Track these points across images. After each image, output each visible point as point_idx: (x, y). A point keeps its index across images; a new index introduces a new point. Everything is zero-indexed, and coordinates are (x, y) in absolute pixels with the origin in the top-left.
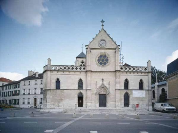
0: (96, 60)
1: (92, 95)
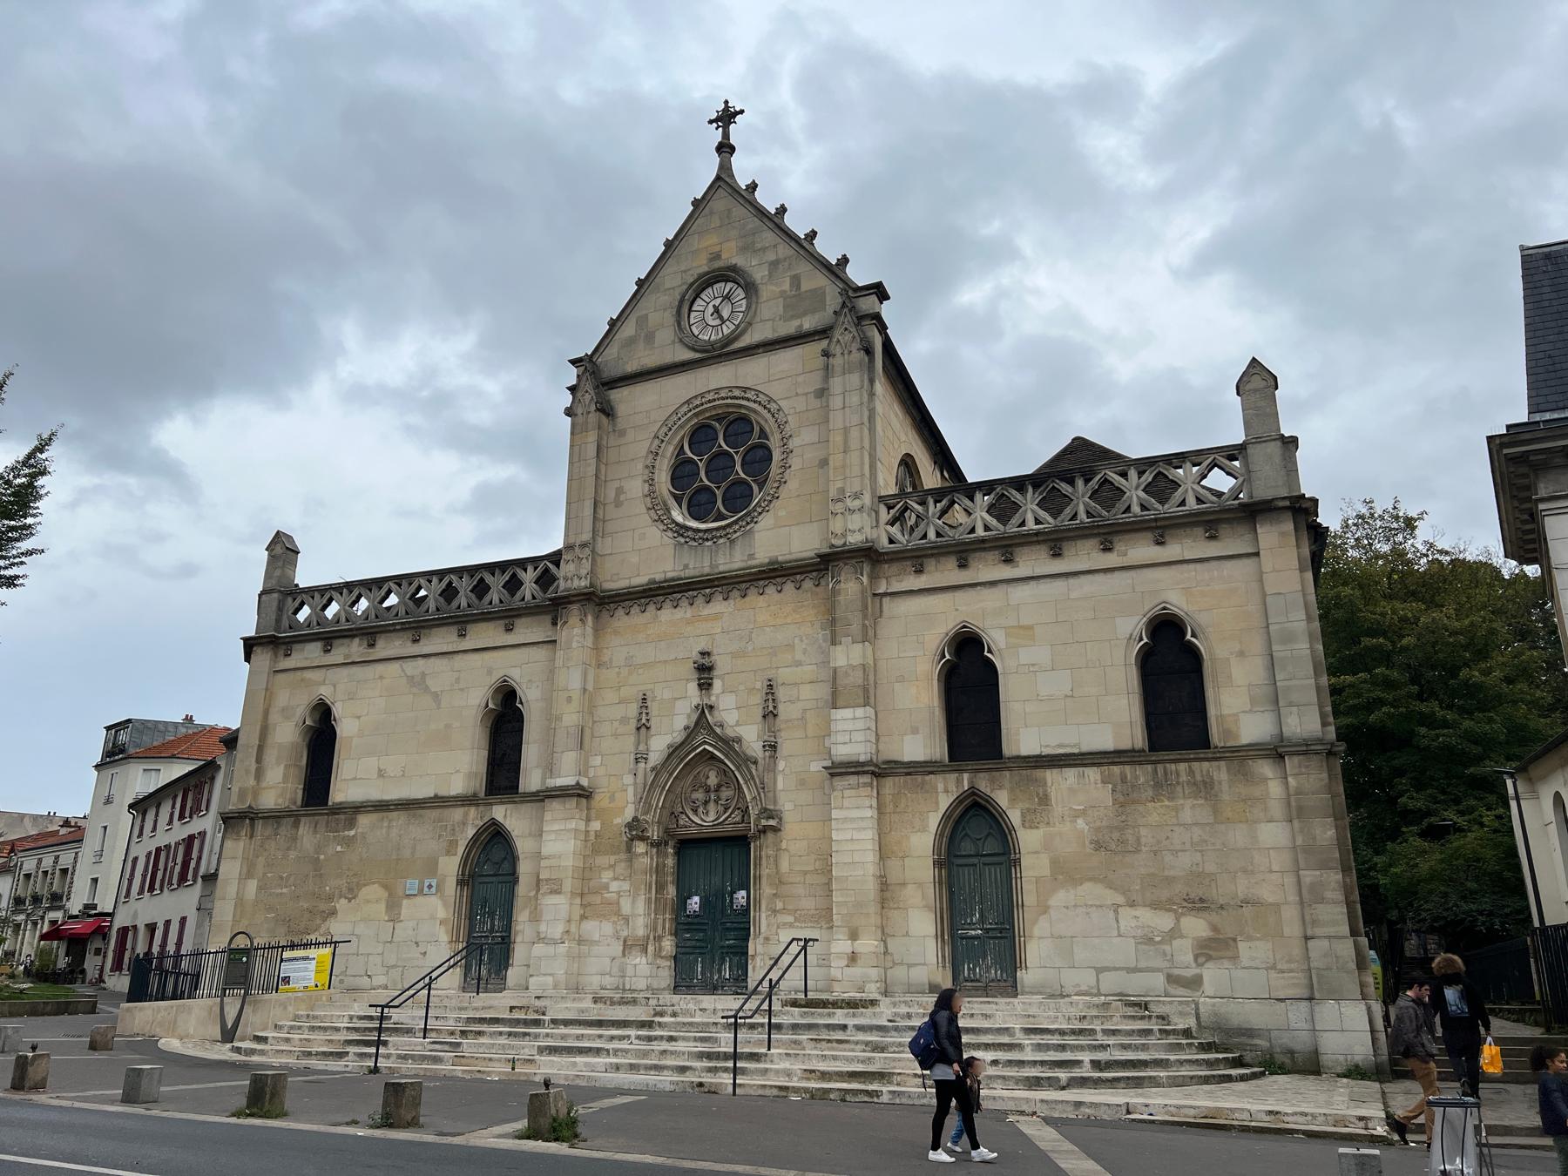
0: (651, 481)
1: (594, 846)
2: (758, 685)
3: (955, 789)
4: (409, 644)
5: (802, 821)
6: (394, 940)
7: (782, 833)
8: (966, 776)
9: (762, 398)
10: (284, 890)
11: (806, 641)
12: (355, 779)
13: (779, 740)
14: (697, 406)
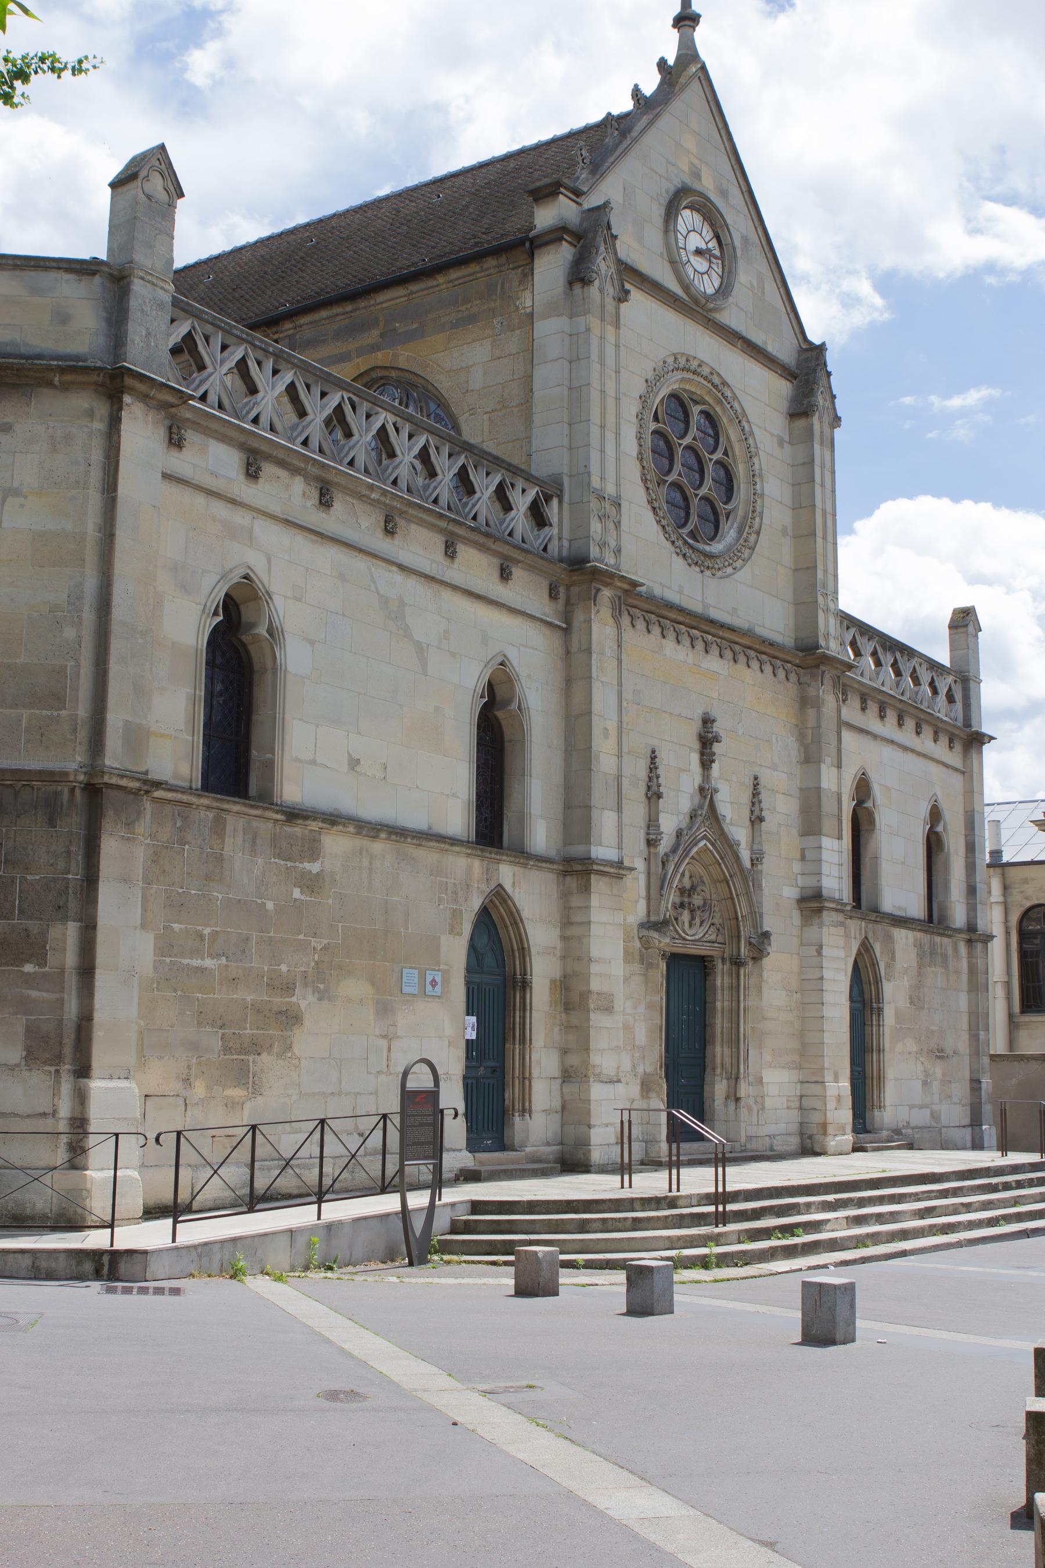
4: (380, 534)
6: (391, 1069)
10: (209, 963)
12: (313, 762)
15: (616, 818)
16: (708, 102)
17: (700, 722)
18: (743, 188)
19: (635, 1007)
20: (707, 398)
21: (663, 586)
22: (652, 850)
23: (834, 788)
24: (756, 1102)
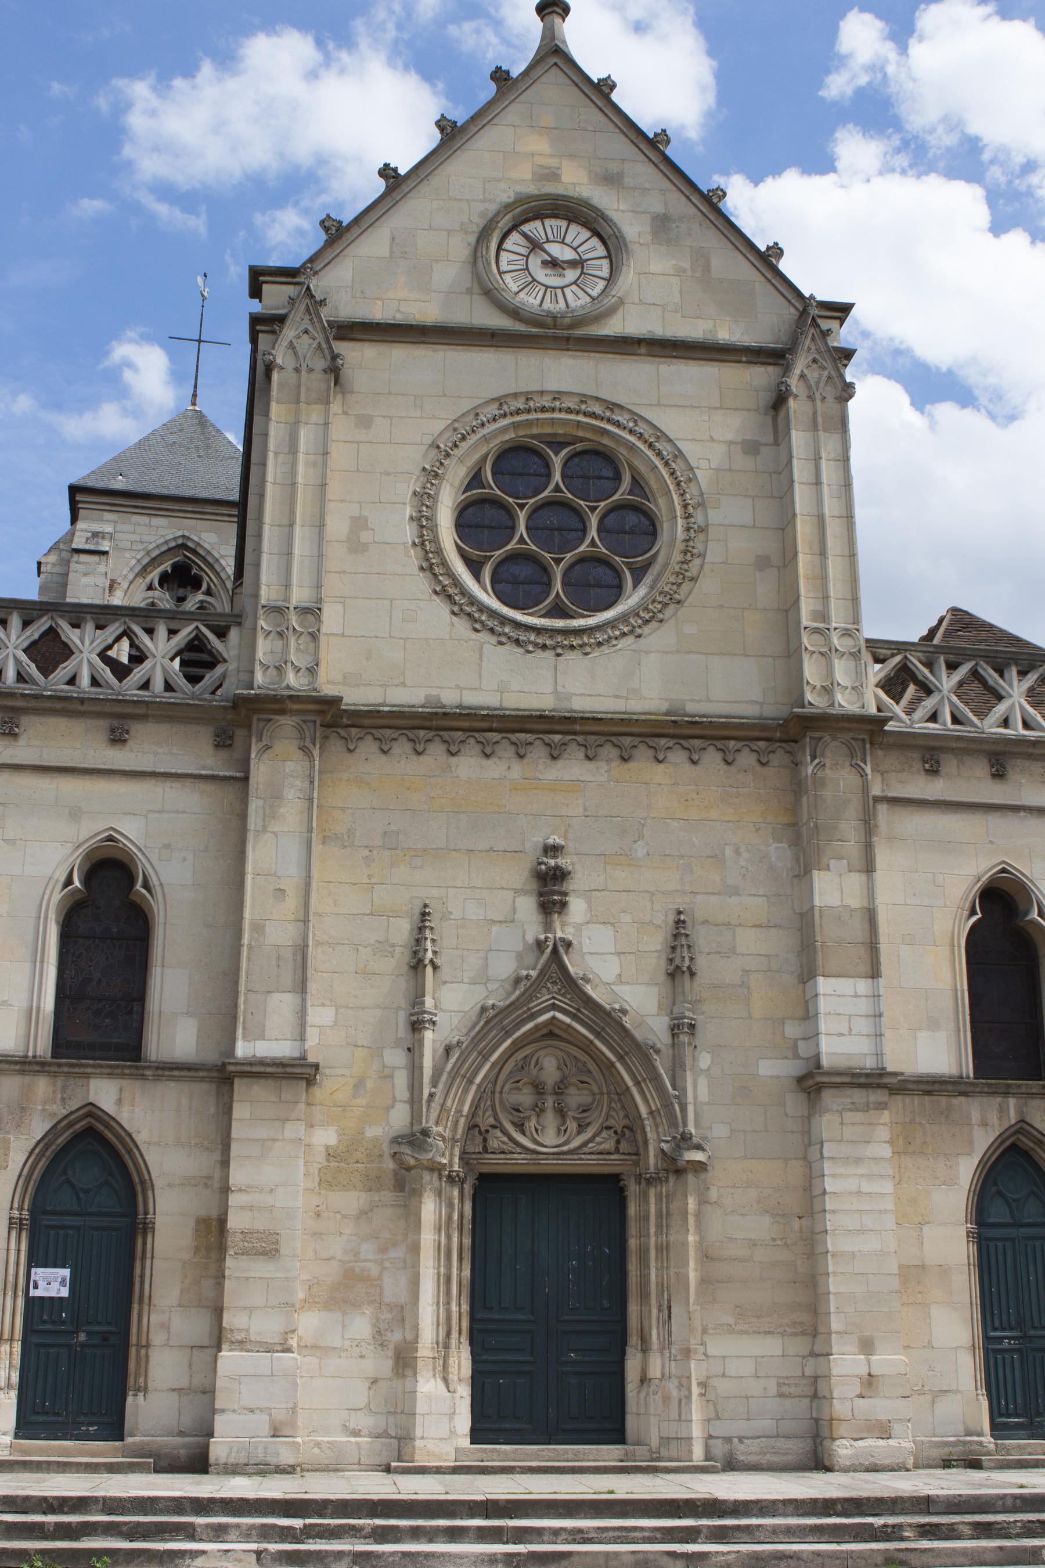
2: (659, 919)
3: (996, 1122)
5: (746, 1157)
7: (710, 1174)
8: (1012, 1102)
9: (642, 428)
11: (746, 855)
13: (700, 1018)
14: (518, 412)
15: (299, 1001)
16: (577, 85)
17: (539, 851)
18: (653, 159)
19: (383, 1250)
20: (581, 434)
21: (461, 689)
22: (417, 1036)
23: (856, 901)
24: (680, 1386)
